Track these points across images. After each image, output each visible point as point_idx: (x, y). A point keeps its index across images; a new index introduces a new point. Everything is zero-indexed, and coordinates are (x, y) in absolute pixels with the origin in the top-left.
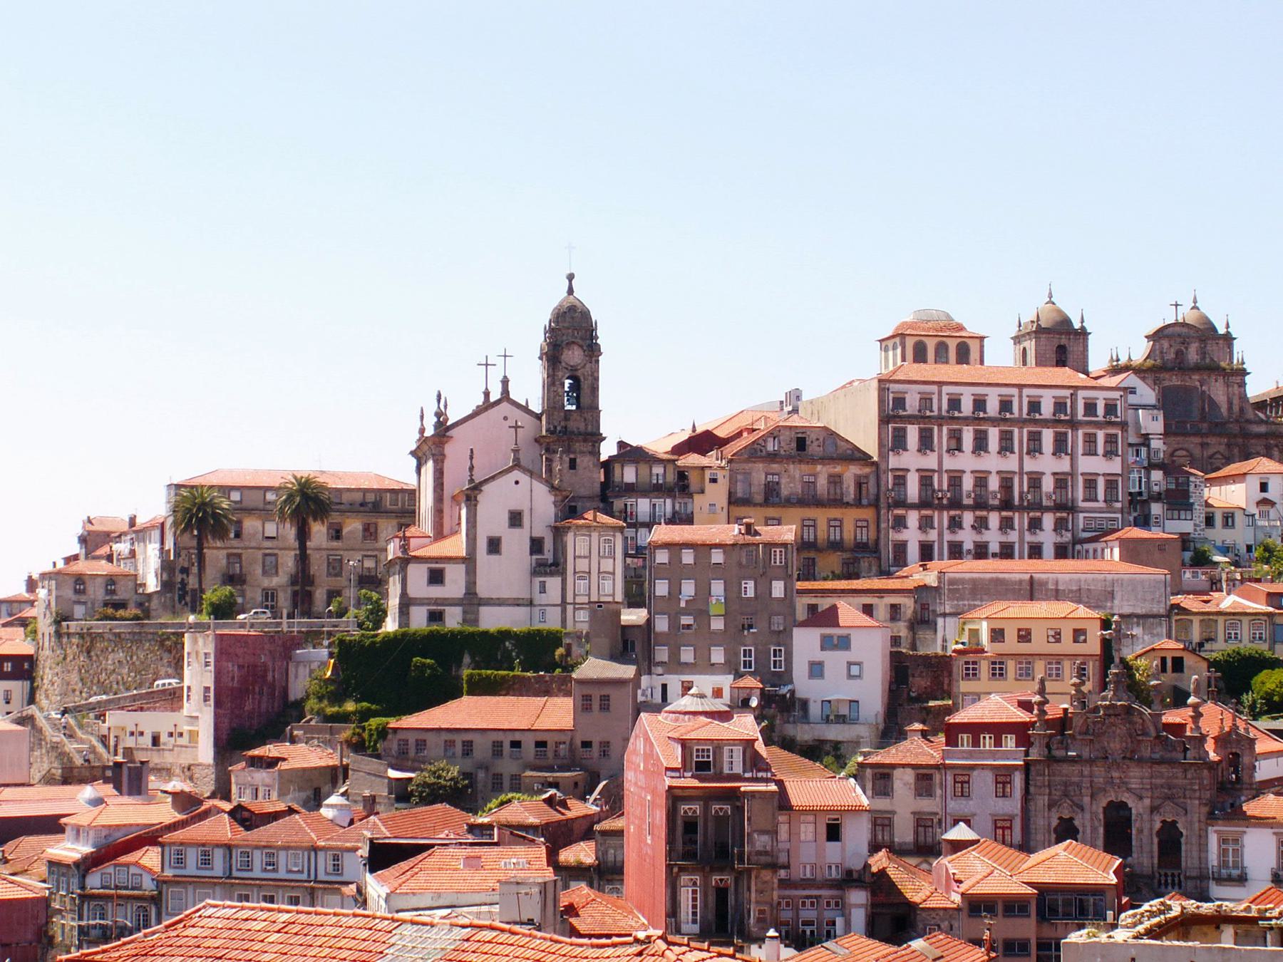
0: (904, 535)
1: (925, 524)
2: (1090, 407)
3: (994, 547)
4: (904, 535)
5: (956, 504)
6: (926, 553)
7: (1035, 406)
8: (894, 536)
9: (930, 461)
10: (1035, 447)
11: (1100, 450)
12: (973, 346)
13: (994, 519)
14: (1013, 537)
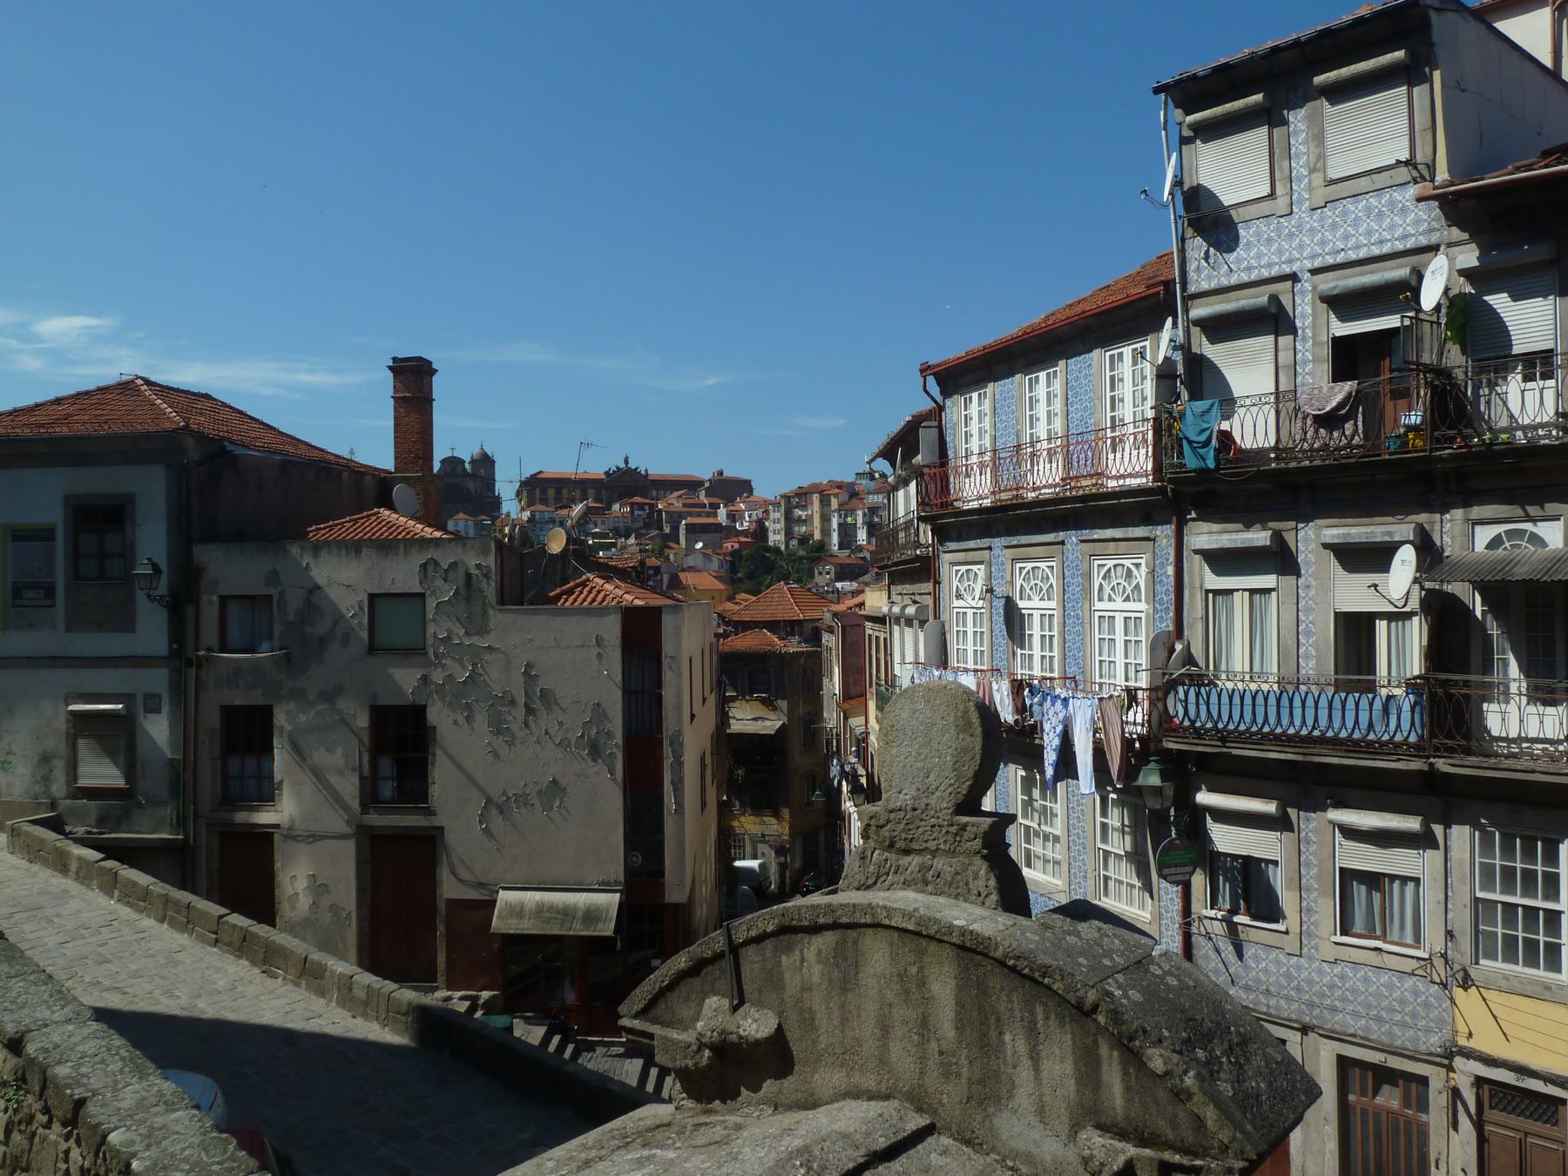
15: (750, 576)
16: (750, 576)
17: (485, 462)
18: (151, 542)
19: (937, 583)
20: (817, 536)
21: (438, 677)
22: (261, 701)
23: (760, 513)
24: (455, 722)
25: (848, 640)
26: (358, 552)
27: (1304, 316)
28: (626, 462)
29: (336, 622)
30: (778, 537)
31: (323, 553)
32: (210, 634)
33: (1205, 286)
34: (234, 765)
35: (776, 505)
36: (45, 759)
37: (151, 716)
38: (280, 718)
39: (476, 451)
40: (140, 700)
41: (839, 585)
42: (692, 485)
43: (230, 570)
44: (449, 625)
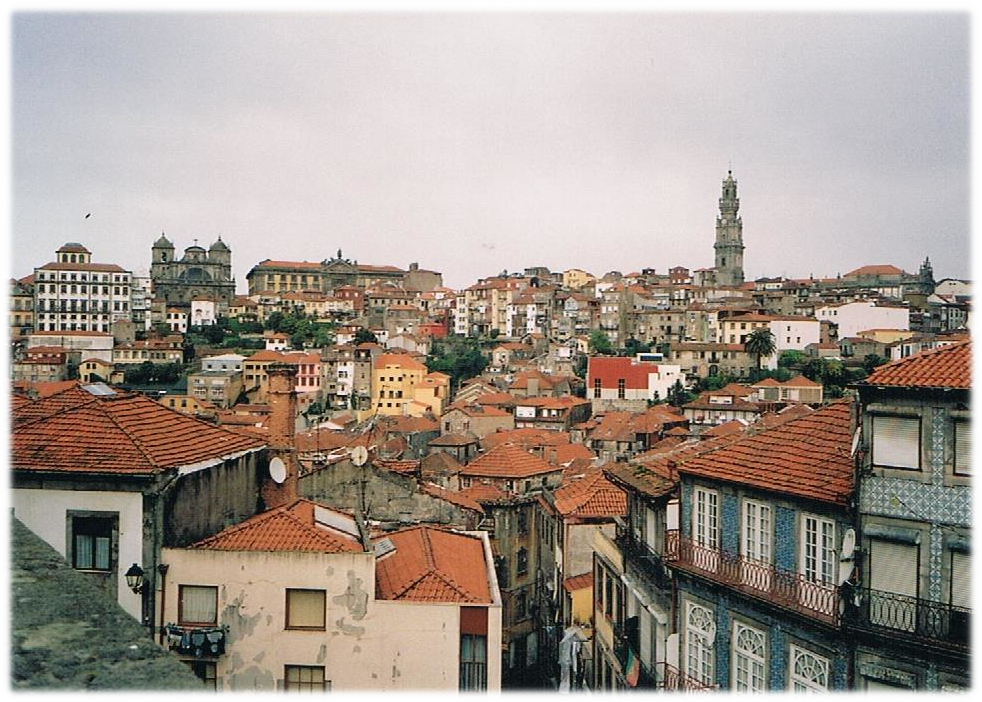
0: (44, 321)
1: (52, 317)
2: (117, 278)
3: (79, 325)
4: (44, 321)
5: (64, 310)
6: (52, 326)
7: (95, 278)
8: (39, 322)
9: (54, 296)
10: (95, 291)
11: (121, 291)
12: (86, 256)
13: (79, 316)
14: (86, 322)
17: (221, 248)
18: (131, 546)
19: (676, 607)
23: (448, 303)
25: (570, 536)
27: (937, 549)
28: (340, 256)
30: (462, 324)
33: (874, 510)
39: (216, 240)
42: (396, 274)
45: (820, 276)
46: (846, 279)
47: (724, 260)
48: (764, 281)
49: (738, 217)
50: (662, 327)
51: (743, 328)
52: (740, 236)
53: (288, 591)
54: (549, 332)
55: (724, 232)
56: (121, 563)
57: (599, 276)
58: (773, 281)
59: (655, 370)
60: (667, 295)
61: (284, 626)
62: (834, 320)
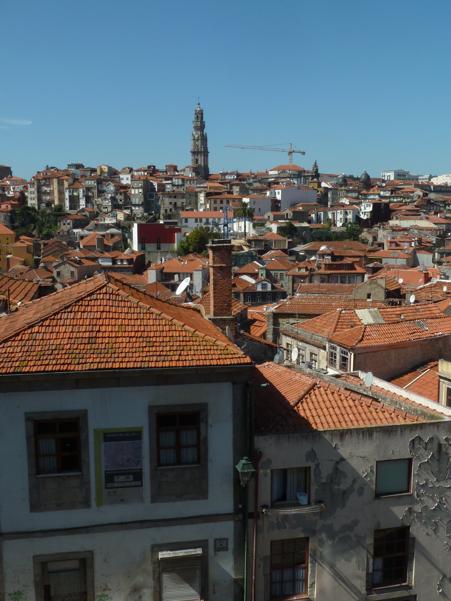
15: (23, 225)
16: (23, 225)
20: (57, 202)
21: (418, 508)
22: (302, 535)
24: (428, 534)
25: (357, 362)
26: (371, 435)
29: (354, 481)
30: (33, 202)
31: (347, 437)
32: (265, 496)
34: (277, 575)
35: (32, 184)
36: (136, 590)
37: (221, 553)
38: (312, 545)
40: (211, 544)
41: (75, 231)
43: (279, 452)
44: (427, 476)
45: (255, 171)
46: (270, 173)
47: (197, 160)
48: (227, 174)
49: (205, 133)
50: (171, 203)
51: (222, 202)
52: (206, 145)
53: (377, 462)
54: (95, 207)
55: (197, 143)
56: (211, 455)
57: (119, 170)
58: (231, 174)
59: (179, 230)
60: (170, 182)
61: (374, 496)
62: (279, 197)
